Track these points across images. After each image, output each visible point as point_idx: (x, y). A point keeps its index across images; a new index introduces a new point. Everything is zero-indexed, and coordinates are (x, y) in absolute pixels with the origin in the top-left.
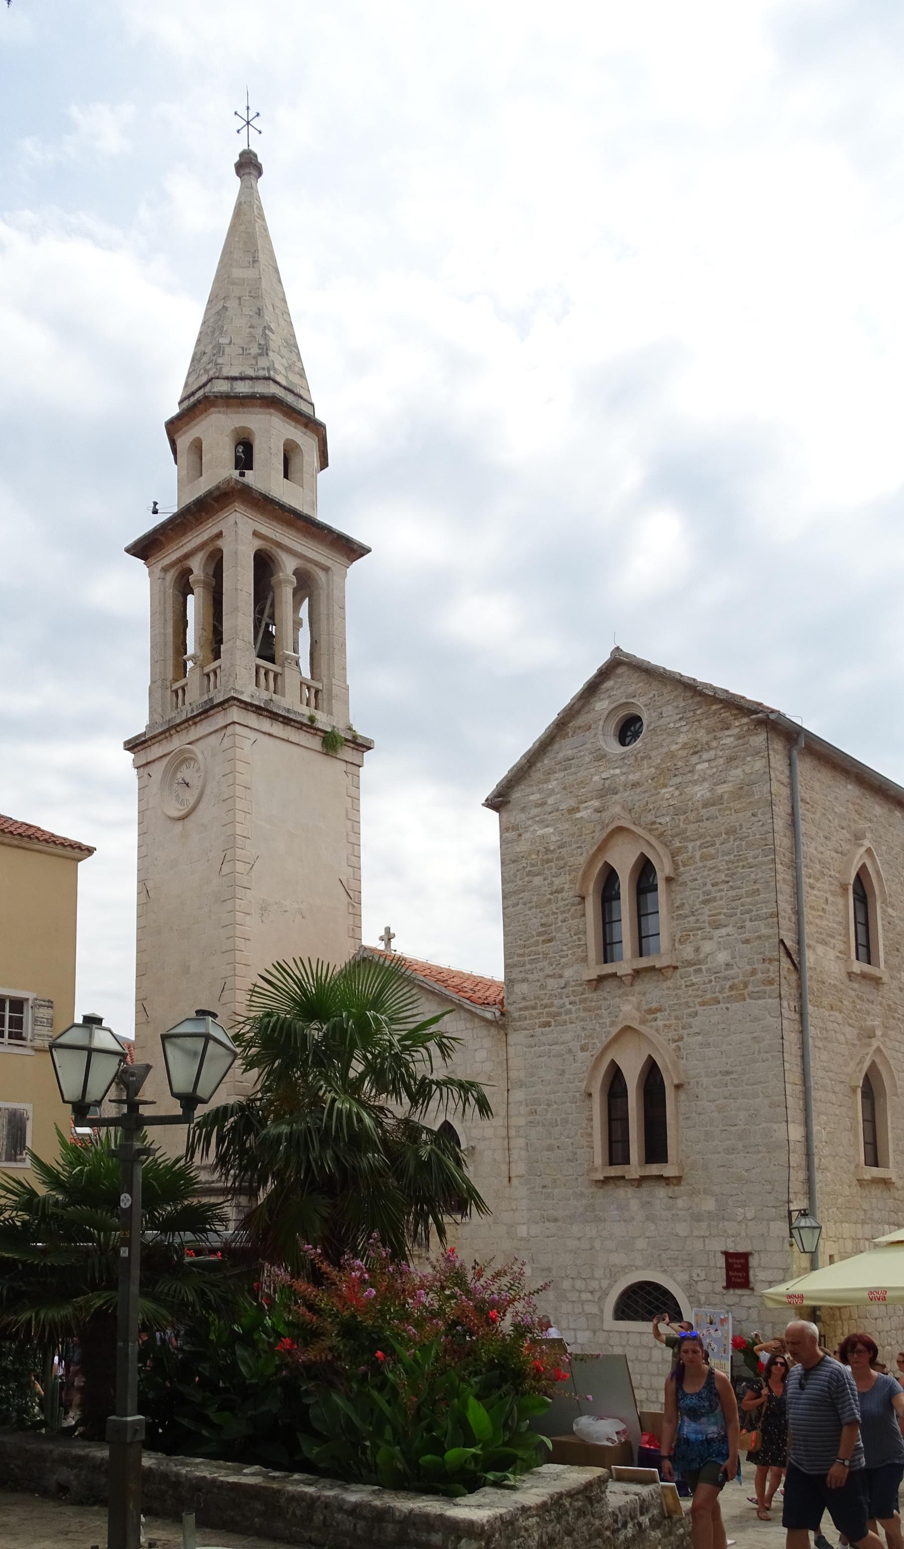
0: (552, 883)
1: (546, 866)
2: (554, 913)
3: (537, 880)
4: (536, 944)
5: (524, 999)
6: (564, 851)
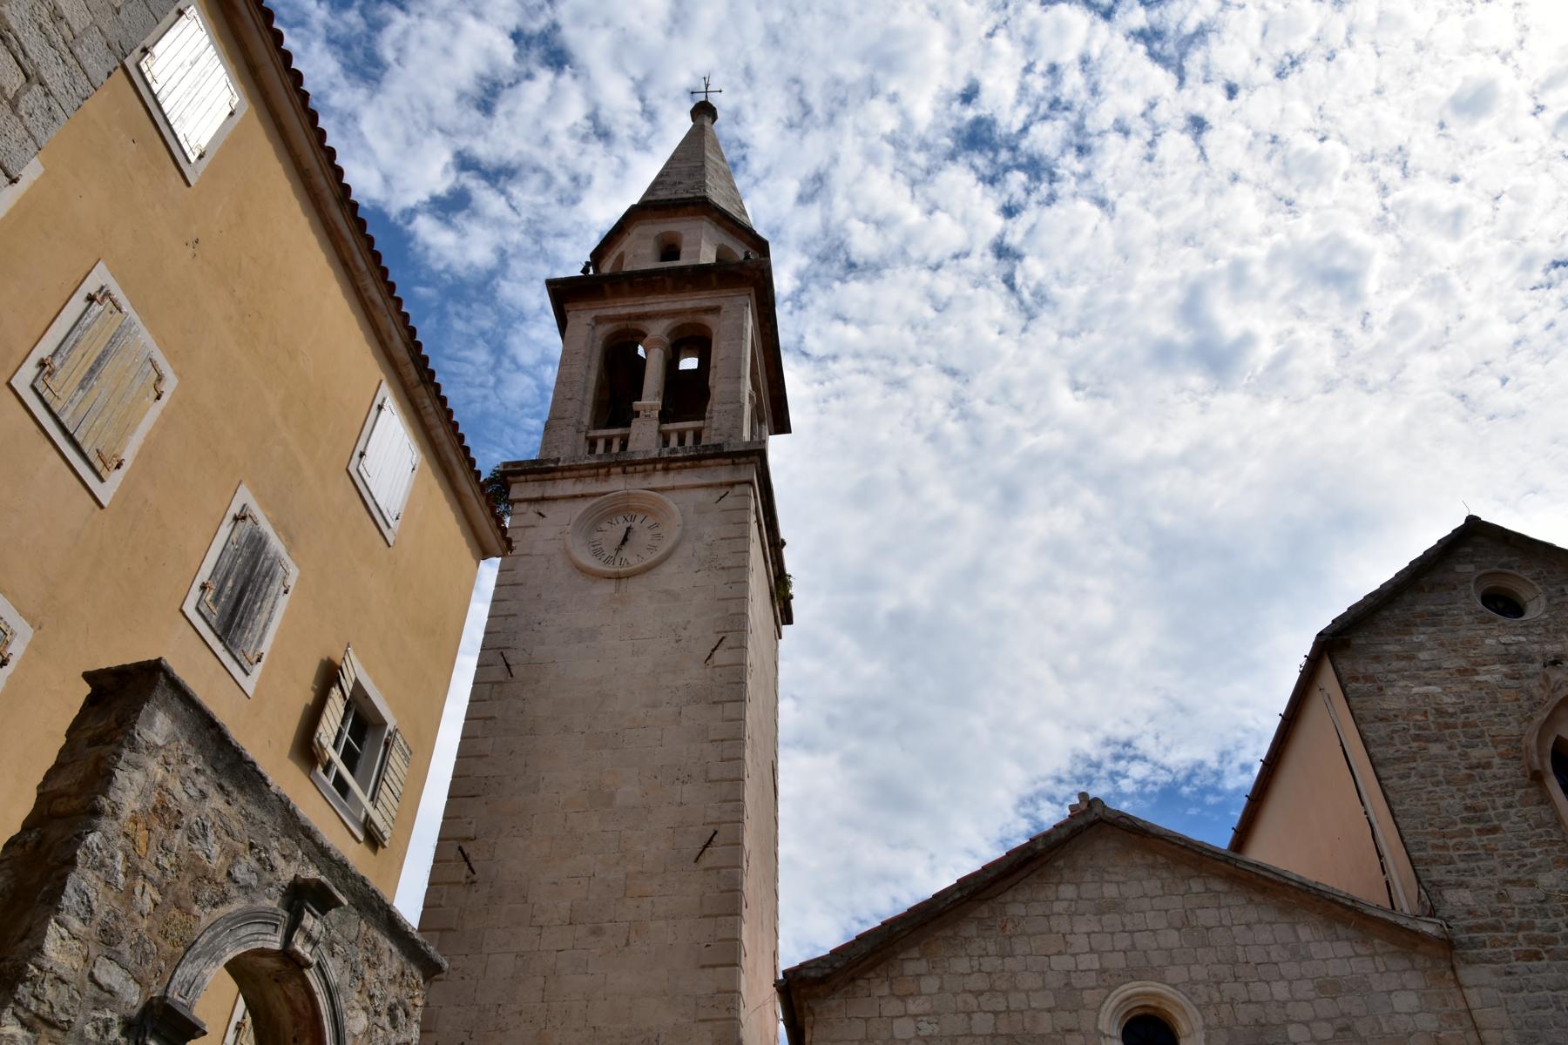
0: (1464, 755)
1: (1447, 732)
2: (1483, 794)
3: (1436, 749)
4: (1466, 833)
5: (1470, 913)
6: (1473, 717)
